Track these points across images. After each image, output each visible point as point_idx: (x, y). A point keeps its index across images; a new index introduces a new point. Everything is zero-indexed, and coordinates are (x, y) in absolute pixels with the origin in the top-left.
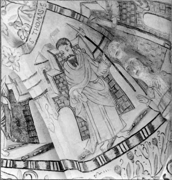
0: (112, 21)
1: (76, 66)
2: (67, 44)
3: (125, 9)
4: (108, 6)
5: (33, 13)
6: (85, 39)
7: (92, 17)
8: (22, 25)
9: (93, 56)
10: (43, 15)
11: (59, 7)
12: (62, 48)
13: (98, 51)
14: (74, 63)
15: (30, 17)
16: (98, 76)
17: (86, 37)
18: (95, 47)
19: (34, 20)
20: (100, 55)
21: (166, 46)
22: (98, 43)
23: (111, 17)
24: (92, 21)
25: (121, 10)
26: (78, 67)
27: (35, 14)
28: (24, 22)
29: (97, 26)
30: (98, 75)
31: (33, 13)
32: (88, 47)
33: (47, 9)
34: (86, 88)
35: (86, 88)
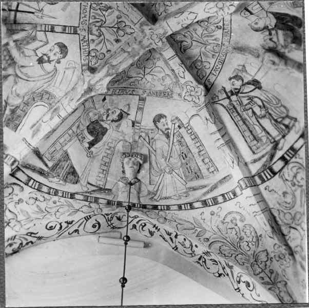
0: (14, 41)
3: (8, 60)
4: (23, 52)
5: (91, 21)
6: (33, 10)
7: (34, 34)
8: (100, 9)
10: (82, 20)
11: (67, 32)
13: (14, 8)
15: (93, 16)
17: (33, 13)
18: (19, 9)
19: (90, 14)
20: (11, 6)
22: (18, 14)
23: (16, 44)
24: (32, 30)
25: (10, 56)
27: (89, 20)
28: (99, 12)
29: (26, 29)
31: (91, 21)
32: (26, 5)
33: (78, 27)
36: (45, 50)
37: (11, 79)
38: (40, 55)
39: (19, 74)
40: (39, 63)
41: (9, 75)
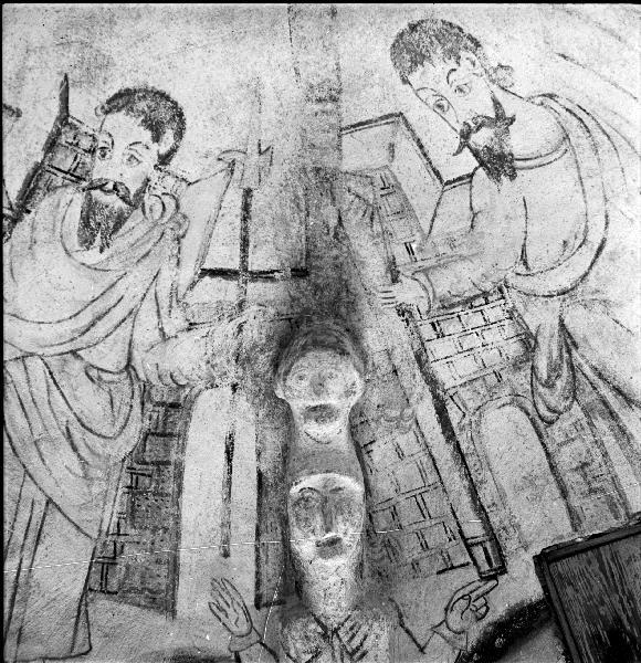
1: (87, 243)
2: (156, 139)
6: (234, 199)
9: (193, 285)
12: (126, 128)
14: (96, 227)
16: (129, 366)
17: (248, 193)
21: (479, 552)
26: (93, 256)
29: (333, 222)
30: (137, 362)
34: (36, 366)
35: (36, 366)
36: (442, 138)
37: (578, 321)
38: (467, 162)
39: (563, 279)
40: (513, 177)
41: (562, 325)
